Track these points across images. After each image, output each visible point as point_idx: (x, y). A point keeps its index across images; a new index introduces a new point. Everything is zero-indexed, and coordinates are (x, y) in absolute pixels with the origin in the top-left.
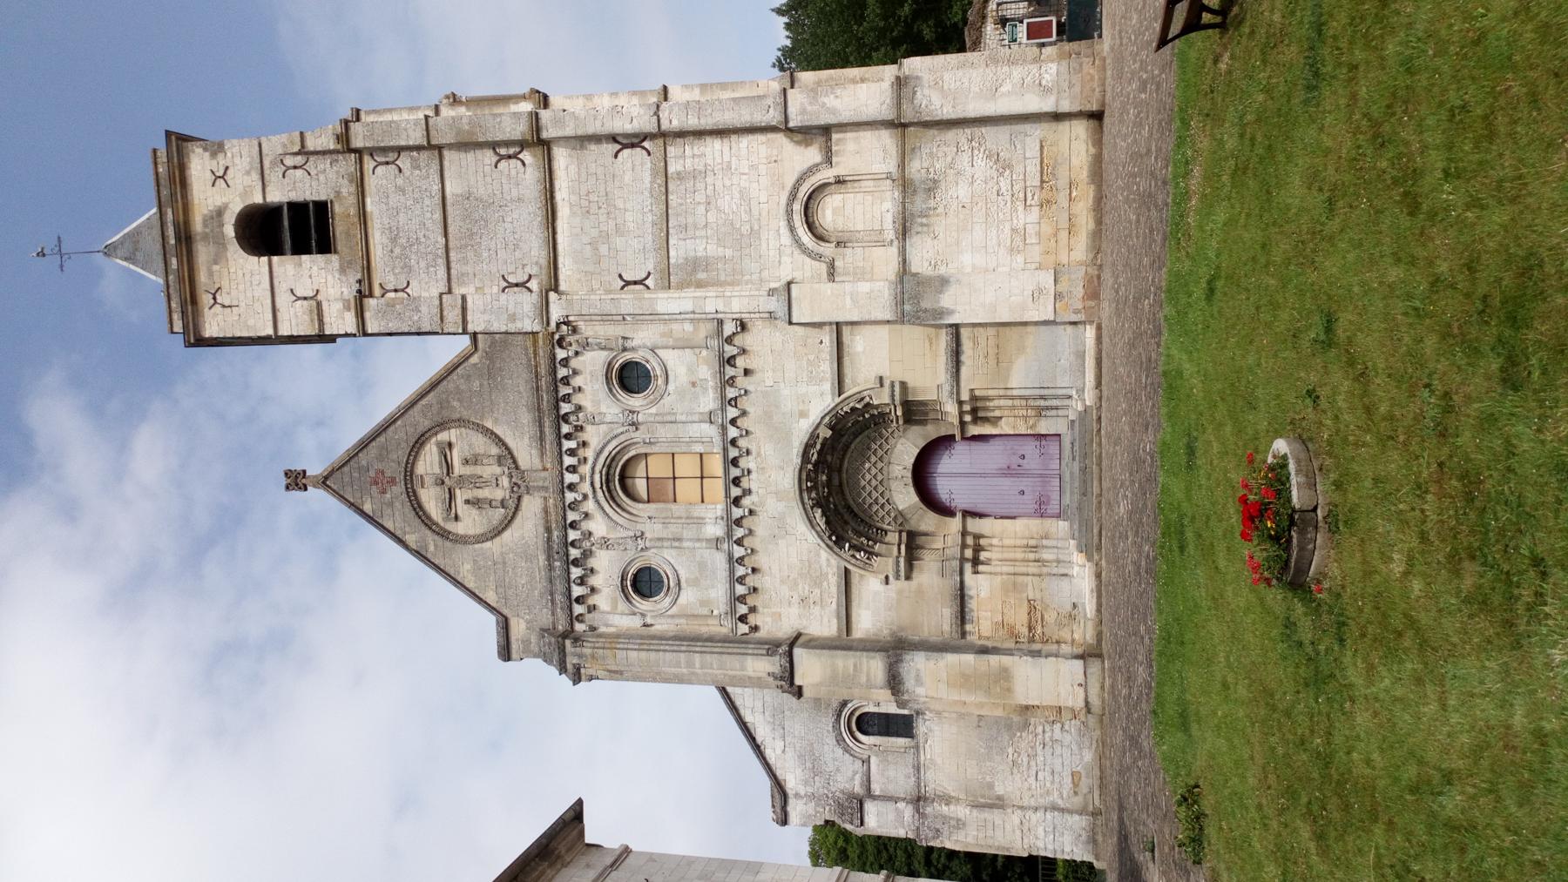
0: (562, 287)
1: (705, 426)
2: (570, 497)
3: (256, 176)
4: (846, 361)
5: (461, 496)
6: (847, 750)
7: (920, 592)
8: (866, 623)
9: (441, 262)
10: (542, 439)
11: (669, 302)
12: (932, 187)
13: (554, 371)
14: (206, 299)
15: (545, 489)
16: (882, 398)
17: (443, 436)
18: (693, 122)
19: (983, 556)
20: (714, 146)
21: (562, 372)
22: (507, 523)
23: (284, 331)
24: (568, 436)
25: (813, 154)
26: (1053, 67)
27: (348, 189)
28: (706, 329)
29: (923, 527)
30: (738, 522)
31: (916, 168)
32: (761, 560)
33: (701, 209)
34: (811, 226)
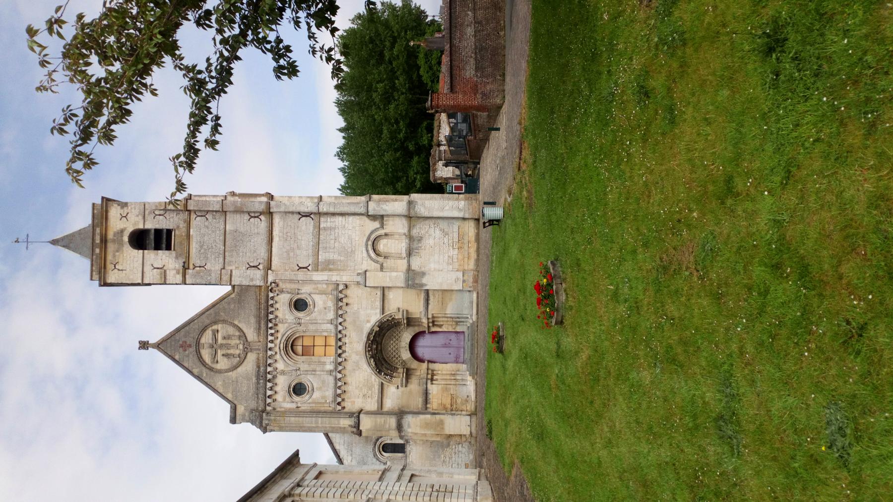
0: (273, 268)
1: (329, 325)
2: (269, 353)
3: (141, 217)
4: (386, 301)
5: (220, 353)
6: (378, 459)
7: (410, 392)
8: (389, 404)
9: (221, 257)
10: (259, 329)
11: (318, 276)
12: (420, 239)
13: (268, 301)
14: (110, 266)
15: (259, 350)
16: (399, 316)
17: (215, 327)
18: (332, 210)
19: (435, 377)
20: (339, 220)
21: (271, 302)
23: (146, 281)
24: (271, 328)
25: (376, 224)
26: (463, 203)
27: (182, 225)
28: (331, 287)
29: (413, 367)
30: (340, 364)
31: (415, 232)
32: (349, 379)
33: (332, 242)
34: (374, 250)
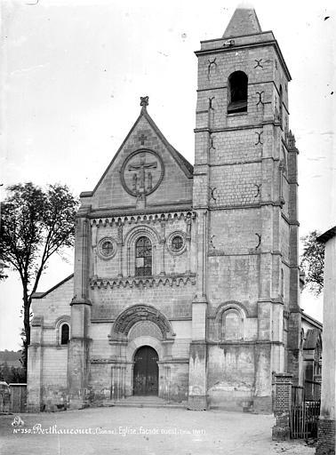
5: (137, 172)
22: (130, 193)
34: (224, 311)
